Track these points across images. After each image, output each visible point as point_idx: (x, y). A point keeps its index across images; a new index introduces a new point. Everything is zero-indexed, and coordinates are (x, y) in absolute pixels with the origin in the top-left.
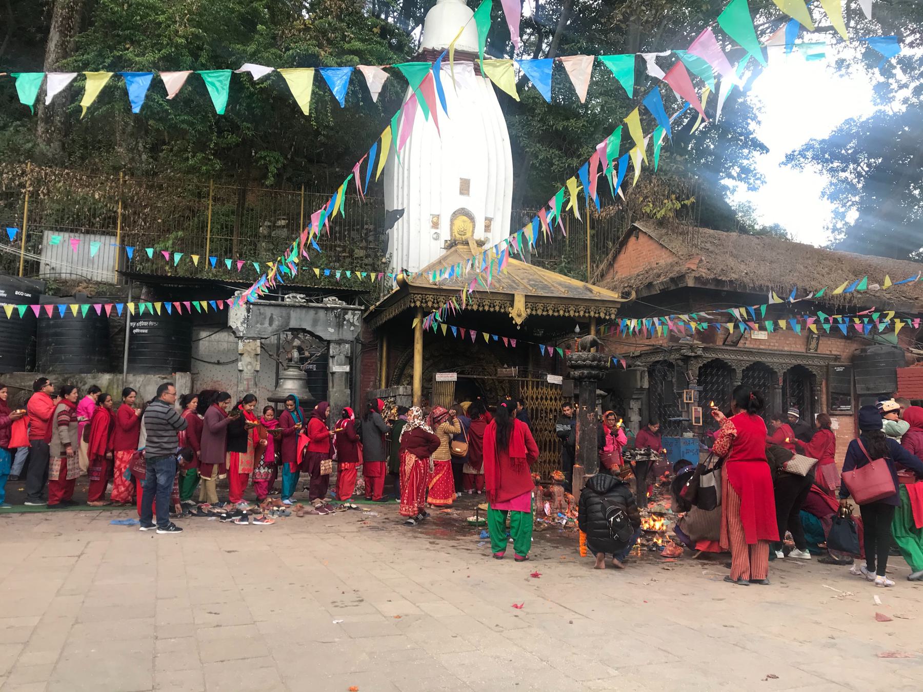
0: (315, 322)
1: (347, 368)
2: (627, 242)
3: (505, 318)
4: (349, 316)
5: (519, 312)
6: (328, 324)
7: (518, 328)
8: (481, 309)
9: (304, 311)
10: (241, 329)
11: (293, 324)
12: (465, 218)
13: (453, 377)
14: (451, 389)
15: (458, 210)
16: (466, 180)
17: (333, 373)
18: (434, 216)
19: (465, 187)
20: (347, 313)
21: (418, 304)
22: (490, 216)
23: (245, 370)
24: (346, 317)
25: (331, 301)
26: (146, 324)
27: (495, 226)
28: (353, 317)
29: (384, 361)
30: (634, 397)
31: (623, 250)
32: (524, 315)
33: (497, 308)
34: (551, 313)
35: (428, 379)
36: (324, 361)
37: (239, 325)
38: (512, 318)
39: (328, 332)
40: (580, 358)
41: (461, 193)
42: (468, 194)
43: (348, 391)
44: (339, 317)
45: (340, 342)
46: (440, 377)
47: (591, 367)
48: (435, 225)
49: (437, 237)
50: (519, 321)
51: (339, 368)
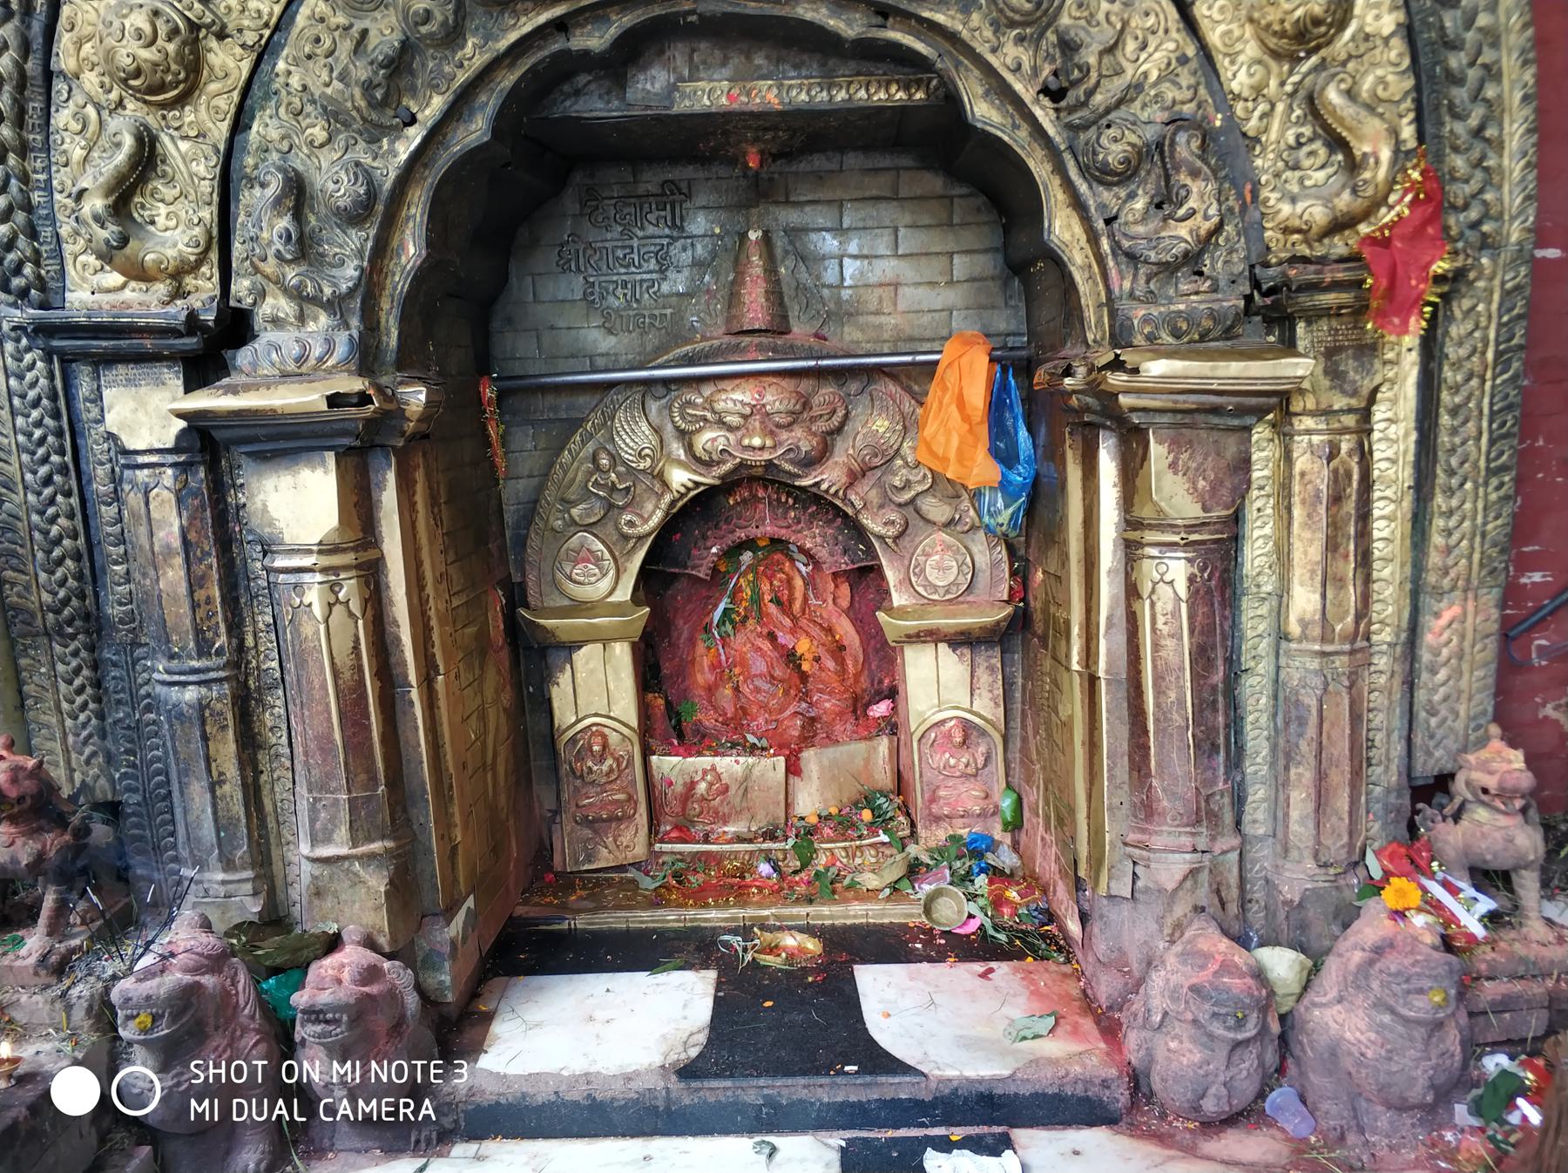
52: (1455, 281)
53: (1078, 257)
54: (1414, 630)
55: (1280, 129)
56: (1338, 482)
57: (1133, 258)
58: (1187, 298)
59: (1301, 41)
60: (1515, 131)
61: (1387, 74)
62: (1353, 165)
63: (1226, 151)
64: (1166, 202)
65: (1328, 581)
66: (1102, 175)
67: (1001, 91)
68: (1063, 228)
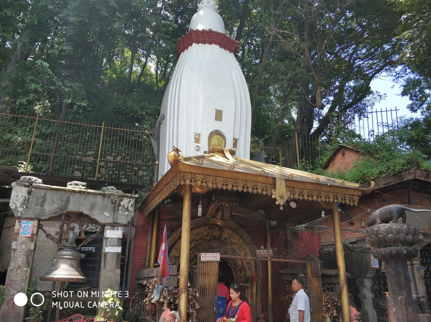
0: (92, 207)
1: (119, 250)
2: (334, 158)
4: (125, 202)
5: (280, 194)
6: (104, 208)
7: (281, 208)
8: (245, 190)
9: (83, 196)
10: (20, 209)
11: (72, 208)
12: (218, 137)
13: (215, 257)
14: (215, 269)
15: (214, 131)
16: (219, 110)
17: (106, 254)
18: (196, 135)
19: (219, 115)
20: (122, 200)
21: (188, 182)
22: (237, 137)
23: (19, 248)
24: (122, 203)
25: (110, 190)
27: (240, 144)
28: (128, 203)
30: (368, 276)
31: (331, 165)
33: (260, 191)
34: (306, 198)
35: (193, 259)
36: (99, 241)
37: (18, 205)
38: (275, 200)
39: (103, 216)
40: (388, 231)
41: (216, 120)
42: (221, 120)
43: (119, 271)
44: (115, 203)
45: (114, 225)
46: (205, 257)
48: (197, 140)
51: (112, 250)
52: (258, 280)
53: (235, 276)
54: (256, 306)
55: (247, 268)
56: (251, 293)
57: (239, 276)
58: (242, 279)
59: (248, 263)
60: (261, 270)
61: (253, 266)
62: (252, 271)
63: (245, 270)
64: (241, 273)
65: (251, 301)
66: (237, 270)
67: (230, 264)
68: (234, 273)
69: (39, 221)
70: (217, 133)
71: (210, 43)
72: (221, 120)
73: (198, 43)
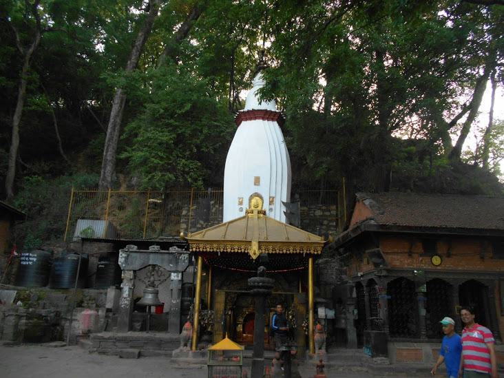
3: (247, 255)
6: (170, 262)
8: (232, 251)
18: (239, 198)
19: (257, 181)
22: (273, 195)
26: (104, 262)
29: (210, 282)
30: (348, 303)
32: (258, 253)
33: (243, 251)
34: (278, 251)
41: (255, 184)
47: (259, 287)
48: (241, 203)
49: (241, 210)
50: (254, 257)
69: (135, 271)
70: (257, 195)
71: (255, 118)
72: (259, 185)
73: (246, 120)
